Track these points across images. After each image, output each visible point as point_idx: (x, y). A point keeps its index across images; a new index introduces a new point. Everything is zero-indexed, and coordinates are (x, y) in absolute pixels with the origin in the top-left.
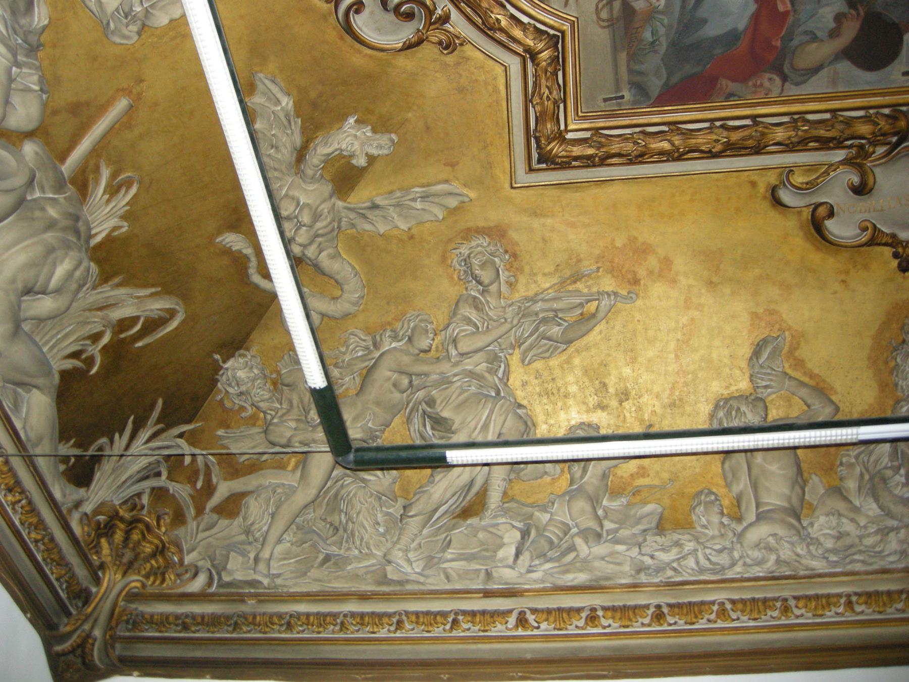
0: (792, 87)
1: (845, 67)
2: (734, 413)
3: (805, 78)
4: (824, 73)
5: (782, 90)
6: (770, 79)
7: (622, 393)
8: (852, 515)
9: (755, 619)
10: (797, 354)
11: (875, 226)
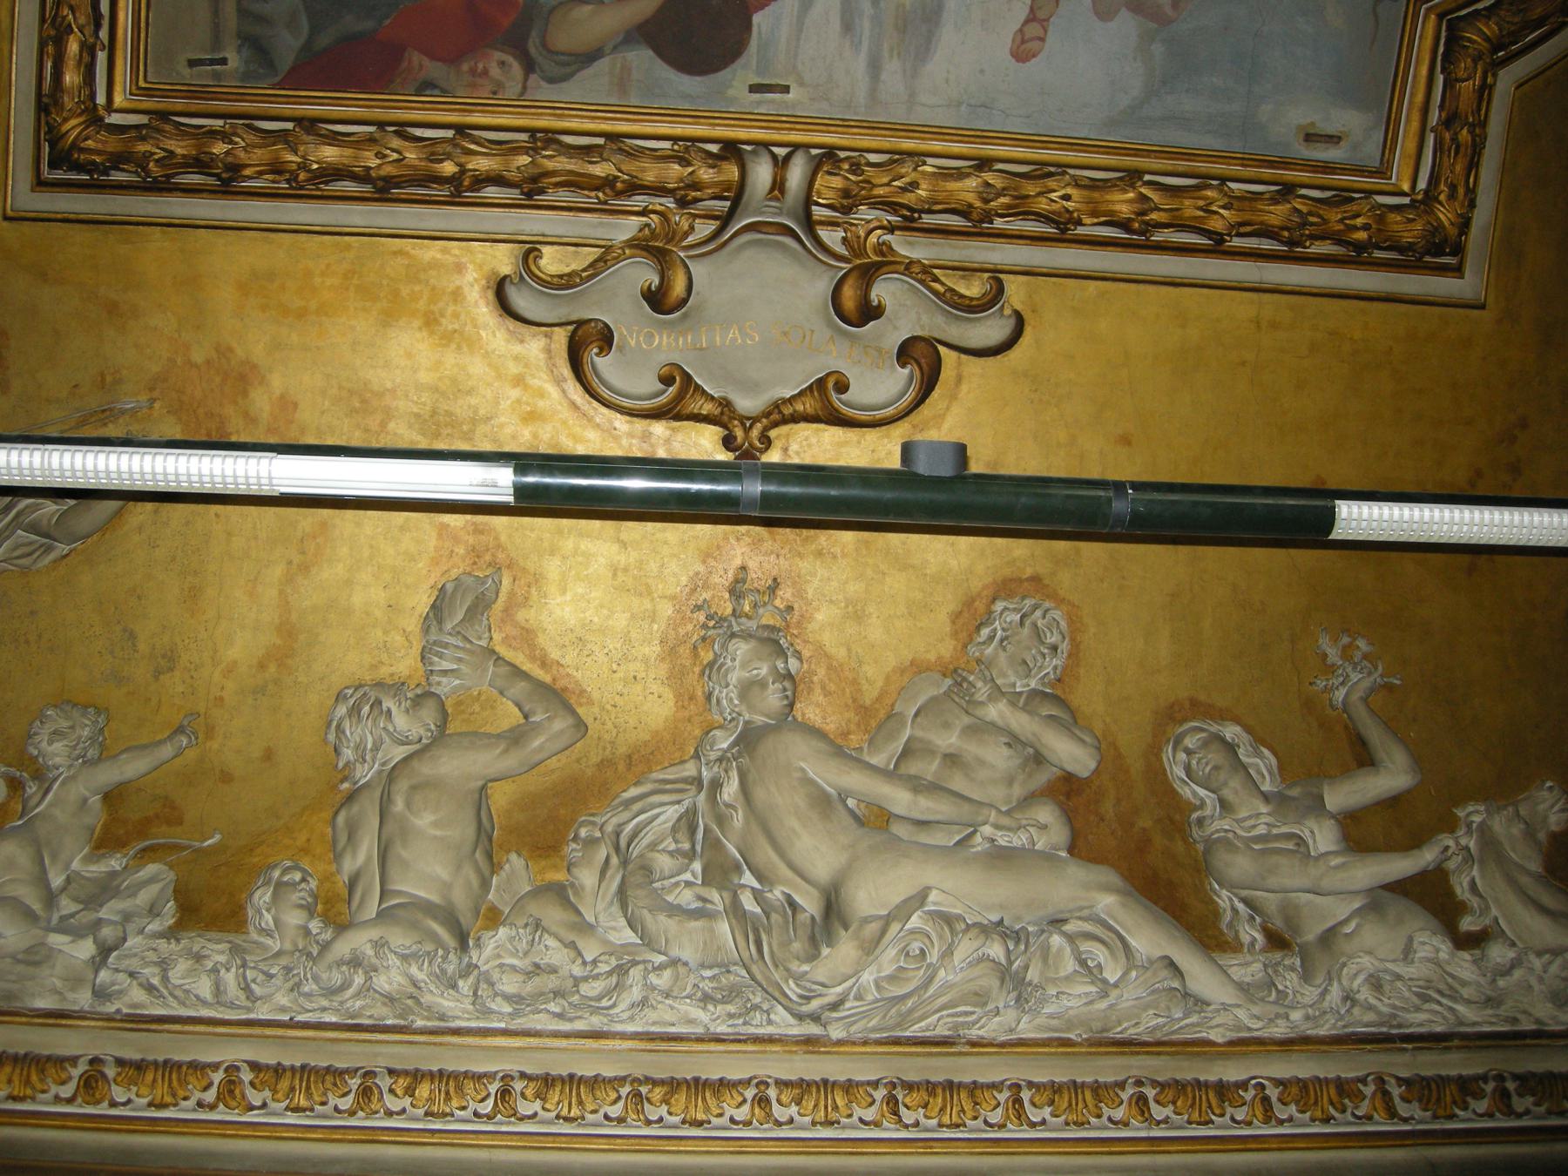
0: (543, 84)
1: (642, 59)
2: (366, 709)
3: (568, 70)
4: (603, 65)
5: (525, 88)
6: (502, 63)
7: (164, 656)
8: (571, 937)
9: (297, 1110)
10: (521, 615)
11: (688, 378)
